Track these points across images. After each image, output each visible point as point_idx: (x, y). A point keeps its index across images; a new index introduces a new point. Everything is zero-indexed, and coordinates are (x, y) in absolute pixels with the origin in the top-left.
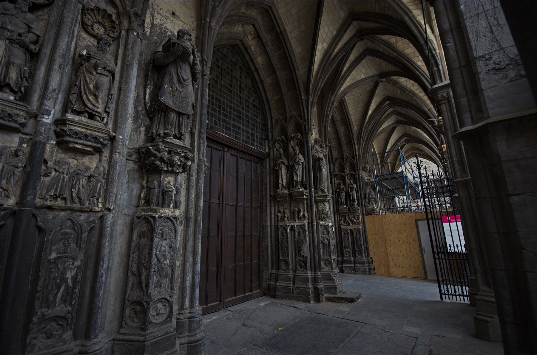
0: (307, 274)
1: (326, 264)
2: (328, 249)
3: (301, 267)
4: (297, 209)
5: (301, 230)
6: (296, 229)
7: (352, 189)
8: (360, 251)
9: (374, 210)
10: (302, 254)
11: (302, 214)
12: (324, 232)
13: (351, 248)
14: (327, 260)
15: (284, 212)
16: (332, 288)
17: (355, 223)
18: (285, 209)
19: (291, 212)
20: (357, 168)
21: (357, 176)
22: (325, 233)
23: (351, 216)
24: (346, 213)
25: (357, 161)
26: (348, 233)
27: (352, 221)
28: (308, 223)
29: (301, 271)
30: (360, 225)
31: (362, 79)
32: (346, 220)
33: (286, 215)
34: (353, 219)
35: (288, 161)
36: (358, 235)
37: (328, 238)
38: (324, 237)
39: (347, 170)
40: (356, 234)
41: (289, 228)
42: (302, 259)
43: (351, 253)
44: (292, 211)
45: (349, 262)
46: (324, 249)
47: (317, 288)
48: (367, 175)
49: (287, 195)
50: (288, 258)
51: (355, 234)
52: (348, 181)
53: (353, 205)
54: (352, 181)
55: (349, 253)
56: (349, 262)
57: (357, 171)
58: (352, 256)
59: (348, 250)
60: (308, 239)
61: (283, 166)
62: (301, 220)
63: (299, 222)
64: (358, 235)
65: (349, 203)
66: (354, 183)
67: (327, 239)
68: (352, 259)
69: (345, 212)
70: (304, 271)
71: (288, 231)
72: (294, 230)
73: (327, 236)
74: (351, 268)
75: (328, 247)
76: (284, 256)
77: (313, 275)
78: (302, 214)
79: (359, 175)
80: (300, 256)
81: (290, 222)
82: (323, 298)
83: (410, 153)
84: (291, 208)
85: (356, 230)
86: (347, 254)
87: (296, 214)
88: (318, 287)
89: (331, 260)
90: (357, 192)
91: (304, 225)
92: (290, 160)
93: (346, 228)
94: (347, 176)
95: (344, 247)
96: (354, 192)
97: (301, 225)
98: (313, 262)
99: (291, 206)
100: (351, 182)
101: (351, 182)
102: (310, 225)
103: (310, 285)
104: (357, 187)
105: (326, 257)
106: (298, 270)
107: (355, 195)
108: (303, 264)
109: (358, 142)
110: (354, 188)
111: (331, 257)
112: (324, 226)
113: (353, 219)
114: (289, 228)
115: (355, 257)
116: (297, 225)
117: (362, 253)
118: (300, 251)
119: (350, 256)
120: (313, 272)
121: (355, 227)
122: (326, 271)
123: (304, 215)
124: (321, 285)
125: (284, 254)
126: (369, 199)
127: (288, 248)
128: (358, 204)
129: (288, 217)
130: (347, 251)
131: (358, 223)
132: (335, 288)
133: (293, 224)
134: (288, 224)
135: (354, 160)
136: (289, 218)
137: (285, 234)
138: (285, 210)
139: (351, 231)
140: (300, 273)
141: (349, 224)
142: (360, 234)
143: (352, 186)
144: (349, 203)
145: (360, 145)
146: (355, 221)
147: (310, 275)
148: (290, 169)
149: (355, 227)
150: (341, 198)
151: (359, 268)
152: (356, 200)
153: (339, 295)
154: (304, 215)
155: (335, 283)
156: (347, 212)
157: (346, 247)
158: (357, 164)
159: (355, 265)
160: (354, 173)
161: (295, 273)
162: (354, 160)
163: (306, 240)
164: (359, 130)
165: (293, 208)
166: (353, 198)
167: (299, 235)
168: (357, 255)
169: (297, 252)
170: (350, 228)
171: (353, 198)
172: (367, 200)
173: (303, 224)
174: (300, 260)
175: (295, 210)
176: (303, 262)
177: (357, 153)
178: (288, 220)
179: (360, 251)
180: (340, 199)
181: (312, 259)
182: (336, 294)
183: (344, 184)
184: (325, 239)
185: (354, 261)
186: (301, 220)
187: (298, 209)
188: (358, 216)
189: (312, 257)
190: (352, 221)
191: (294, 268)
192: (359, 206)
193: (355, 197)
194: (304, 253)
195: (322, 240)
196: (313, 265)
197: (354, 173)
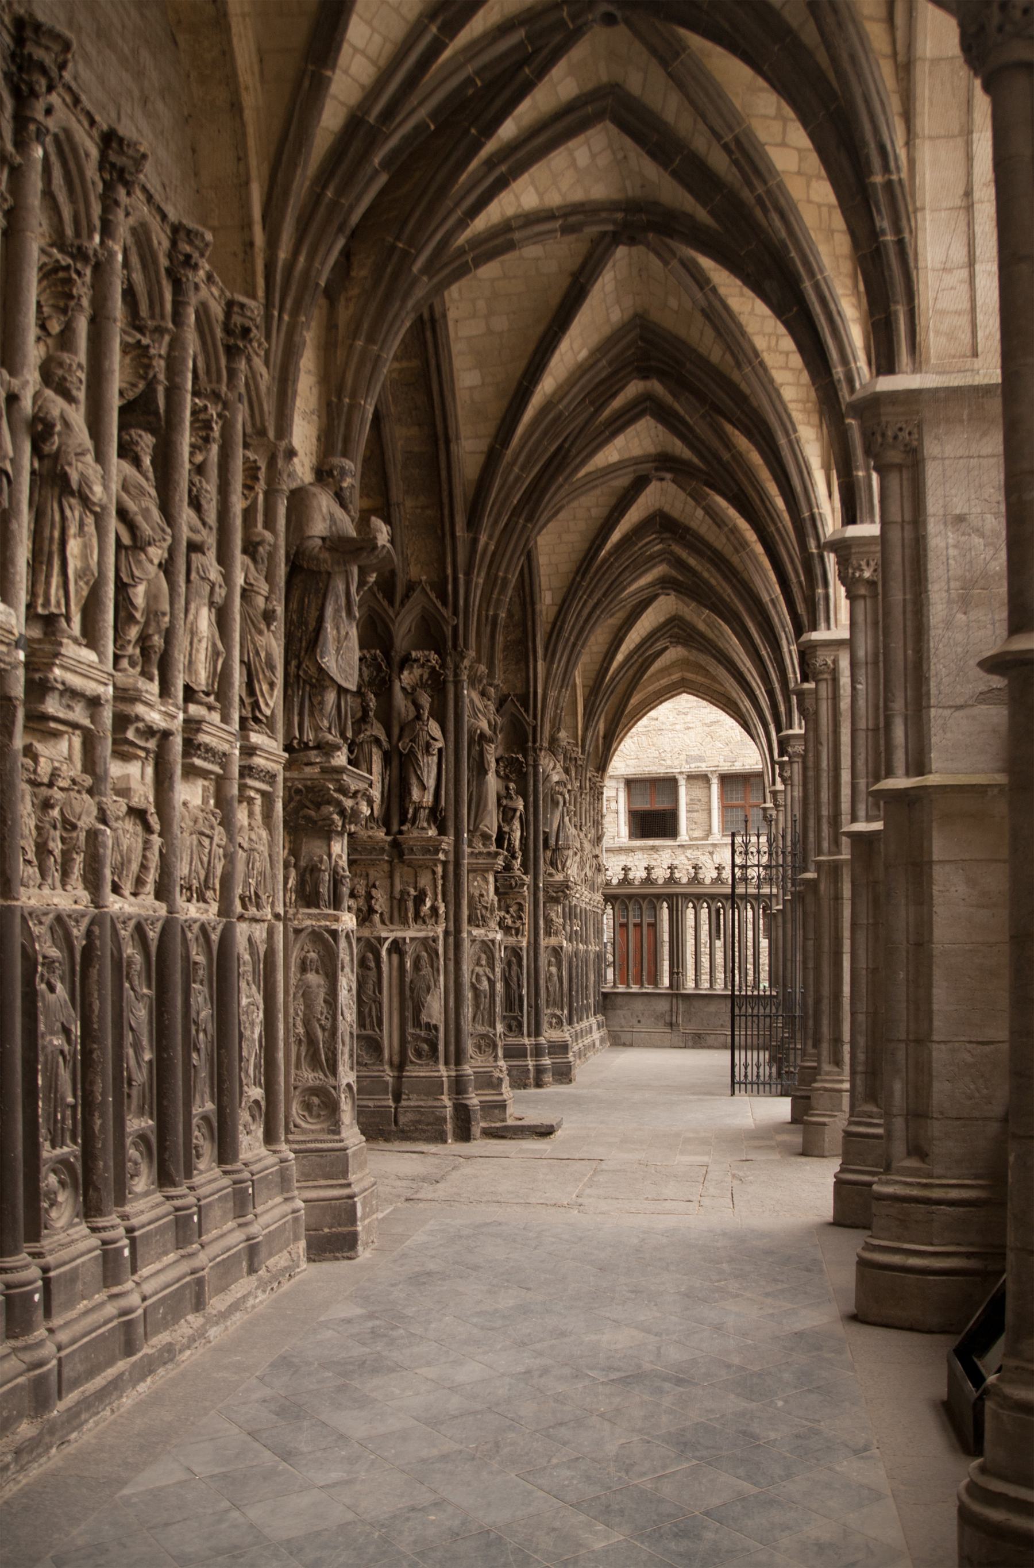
0: (438, 1071)
1: (479, 1047)
2: (487, 1006)
3: (419, 1054)
4: (412, 892)
5: (424, 954)
6: (410, 949)
7: (510, 814)
8: (515, 1018)
9: (568, 887)
10: (424, 1018)
11: (428, 904)
12: (479, 959)
14: (483, 1036)
15: (369, 897)
16: (495, 1107)
18: (374, 886)
19: (392, 897)
21: (531, 769)
22: (484, 962)
25: (535, 717)
28: (446, 933)
29: (421, 1065)
30: (523, 935)
31: (609, 466)
33: (377, 907)
35: (389, 735)
36: (515, 967)
37: (491, 976)
38: (481, 973)
41: (386, 945)
42: (423, 1033)
44: (398, 896)
46: (477, 1006)
47: (466, 1106)
49: (387, 847)
50: (381, 1030)
54: (512, 785)
57: (531, 753)
60: (442, 978)
61: (374, 750)
62: (424, 922)
63: (421, 930)
64: (515, 967)
66: (517, 793)
67: (489, 979)
70: (427, 1065)
71: (384, 953)
72: (401, 954)
73: (487, 970)
75: (487, 1000)
76: (368, 1026)
77: (453, 1074)
78: (428, 904)
79: (536, 767)
80: (417, 1023)
81: (391, 927)
82: (476, 1130)
83: (675, 677)
84: (392, 885)
87: (410, 905)
88: (468, 1102)
89: (495, 1035)
90: (524, 825)
91: (435, 940)
92: (396, 731)
96: (517, 824)
97: (426, 939)
98: (452, 1040)
99: (391, 876)
100: (507, 788)
101: (507, 788)
102: (451, 939)
103: (446, 1101)
104: (525, 807)
105: (482, 1029)
106: (412, 1062)
107: (518, 834)
108: (426, 1047)
109: (546, 649)
110: (515, 810)
111: (495, 1028)
112: (483, 942)
114: (386, 945)
116: (412, 939)
117: (520, 1025)
118: (418, 1009)
120: (452, 1066)
122: (480, 1064)
123: (434, 909)
124: (474, 1099)
125: (368, 1021)
127: (380, 1004)
129: (381, 914)
131: (517, 930)
132: (502, 1106)
133: (399, 934)
134: (384, 935)
135: (527, 711)
136: (386, 917)
137: (372, 964)
138: (374, 892)
140: (417, 1071)
142: (520, 966)
143: (511, 804)
145: (552, 662)
147: (445, 1074)
148: (395, 763)
153: (510, 1122)
154: (434, 909)
155: (502, 1094)
158: (535, 728)
160: (520, 756)
161: (402, 1071)
162: (527, 711)
163: (436, 981)
164: (556, 609)
165: (398, 887)
167: (417, 966)
169: (409, 1014)
173: (431, 934)
174: (417, 1037)
175: (404, 893)
176: (426, 1041)
177: (540, 691)
178: (383, 922)
181: (452, 1033)
182: (504, 1120)
184: (484, 978)
186: (424, 922)
187: (415, 889)
189: (452, 1026)
191: (396, 1059)
192: (526, 873)
193: (517, 843)
194: (430, 1016)
195: (474, 980)
196: (452, 1048)
197: (520, 756)
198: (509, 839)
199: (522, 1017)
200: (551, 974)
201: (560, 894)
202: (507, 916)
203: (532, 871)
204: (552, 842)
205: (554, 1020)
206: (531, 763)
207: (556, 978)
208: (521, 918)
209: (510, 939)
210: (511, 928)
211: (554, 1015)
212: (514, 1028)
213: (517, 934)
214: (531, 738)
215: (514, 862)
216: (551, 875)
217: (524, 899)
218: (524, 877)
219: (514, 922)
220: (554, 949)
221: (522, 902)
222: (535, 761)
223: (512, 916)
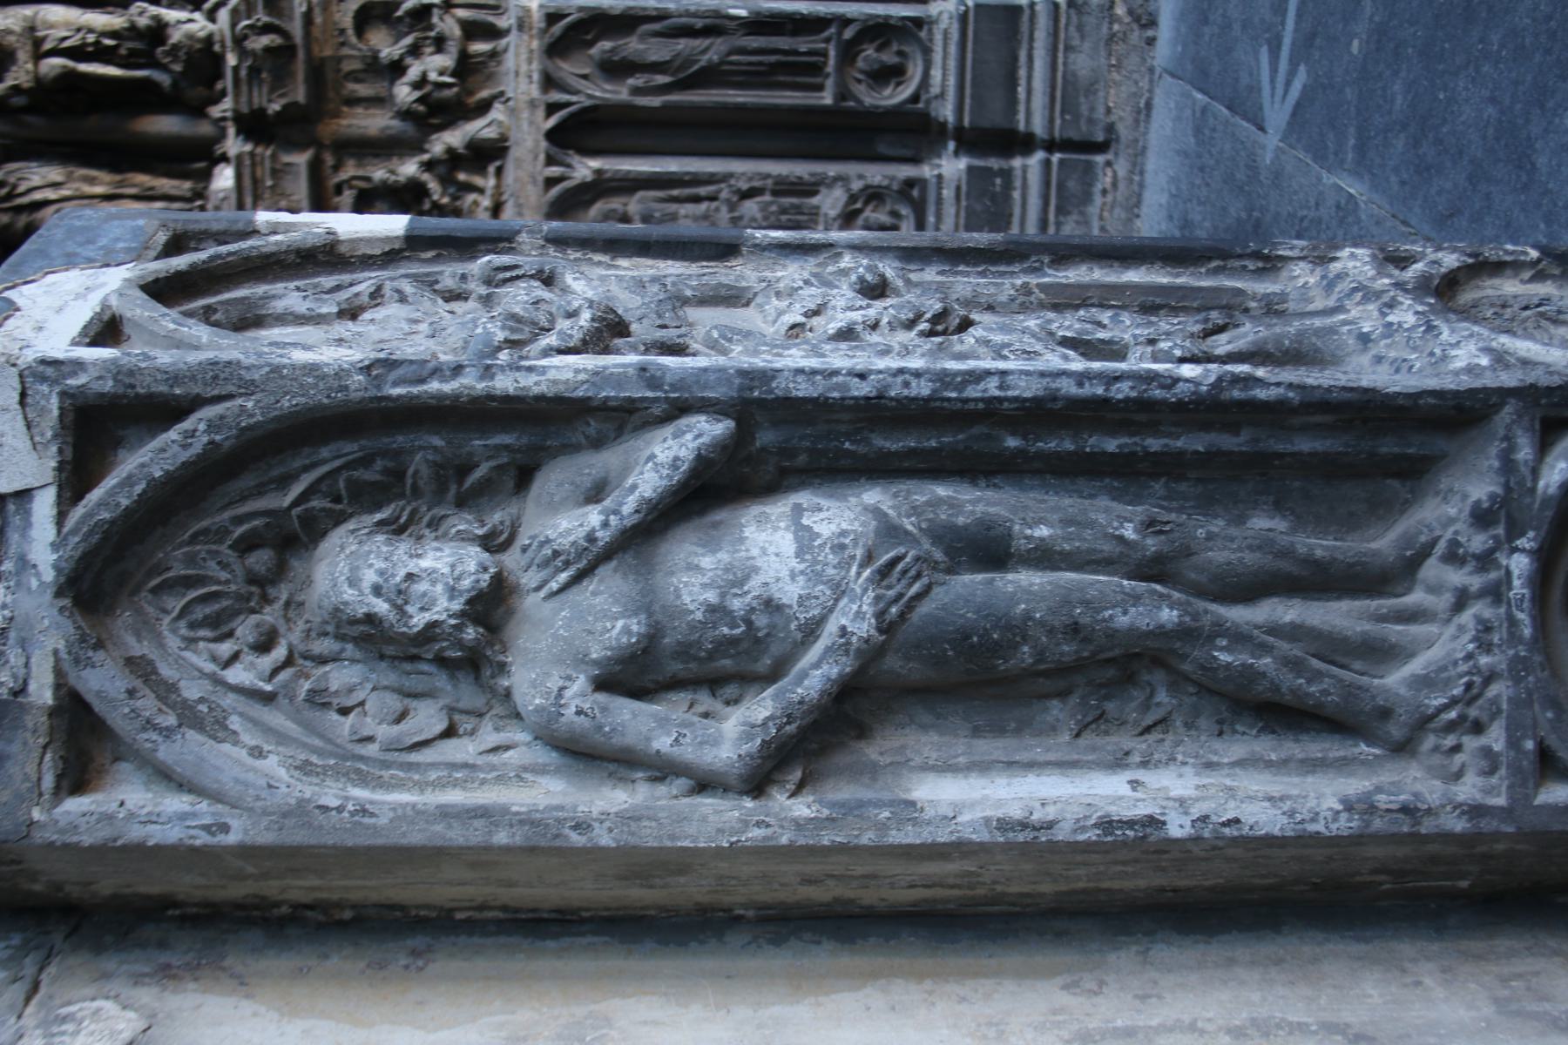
8: (849, 53)
13: (800, 169)
17: (466, 68)
23: (375, 122)
26: (600, 187)
36: (633, 46)
40: (615, 69)
43: (876, 174)
51: (618, 92)
58: (905, 171)
64: (633, 46)
65: (166, 125)
68: (951, 166)
85: (568, 69)
113: (404, 93)
141: (487, 154)
144: (166, 125)
146: (435, 65)
151: (1067, 92)
156: (301, 159)
159: (1024, 143)
166: (99, 53)
168: (894, 96)
171: (99, 53)
179: (849, 53)
185: (972, 140)
198: (77, 53)
199: (845, 21)
202: (414, 72)
209: (510, 61)
210: (464, 58)
212: (889, 58)
213: (493, 33)
215: (176, 36)
219: (440, 44)
223: (415, 51)
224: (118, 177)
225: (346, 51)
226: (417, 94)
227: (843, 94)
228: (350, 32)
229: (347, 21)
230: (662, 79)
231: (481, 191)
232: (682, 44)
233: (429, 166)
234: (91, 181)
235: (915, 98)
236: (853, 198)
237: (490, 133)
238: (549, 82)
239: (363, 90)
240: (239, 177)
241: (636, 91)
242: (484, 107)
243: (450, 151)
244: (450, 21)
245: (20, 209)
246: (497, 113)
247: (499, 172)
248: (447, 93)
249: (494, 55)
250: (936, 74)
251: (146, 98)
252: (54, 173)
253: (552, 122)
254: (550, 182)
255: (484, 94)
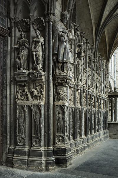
8: (38, 138)
20: (48, 10)
23: (31, 87)
24: (25, 81)
26: (24, 111)
27: (32, 93)
30: (42, 100)
32: (24, 91)
34: (33, 90)
36: (38, 114)
39: (35, 14)
40: (36, 113)
45: (23, 153)
48: (63, 26)
51: (33, 113)
52: (33, 33)
53: (35, 69)
55: (24, 140)
56: (23, 153)
57: (47, 16)
59: (23, 136)
64: (38, 114)
65: (31, 66)
66: (42, 35)
69: (23, 79)
74: (23, 162)
86: (20, 141)
93: (23, 104)
94: (33, 24)
95: (17, 132)
104: (45, 41)
107: (41, 53)
115: (31, 145)
117: (40, 141)
119: (24, 145)
121: (36, 102)
126: (64, 63)
128: (44, 69)
130: (22, 138)
131: (40, 97)
139: (29, 108)
142: (40, 114)
146: (36, 93)
149: (36, 102)
150: (20, 59)
152: (41, 62)
156: (26, 79)
157: (20, 131)
160: (42, 18)
170: (28, 103)
172: (60, 65)
179: (38, 138)
180: (18, 60)
183: (28, 37)
188: (42, 87)
190: (32, 93)
192: (44, 71)
197: (42, 18)
199: (41, 137)
200: (59, 118)
201: (63, 81)
202: (35, 91)
203: (47, 70)
204: (61, 58)
205: (61, 138)
206: (47, 21)
207: (61, 120)
208: (41, 91)
211: (61, 136)
213: (40, 99)
214: (46, 9)
216: (60, 74)
217: (43, 83)
218: (43, 73)
219: (38, 93)
220: (61, 106)
221: (42, 84)
222: (49, 19)
223: (38, 91)
224: (26, 60)
225: (38, 84)
226: (33, 91)
227: (33, 137)
228: (39, 84)
229: (40, 84)
230: (35, 117)
231: (24, 98)
232: (38, 120)
233: (27, 93)
234: (25, 57)
235: (33, 145)
236: (24, 138)
237: (29, 99)
238: (34, 105)
239: (35, 85)
240: (24, 73)
241: (33, 115)
242: (32, 99)
243: (28, 95)
244: (40, 95)
245: (21, 50)
246: (31, 99)
247: (26, 100)
248: (33, 94)
249: (38, 99)
250: (36, 147)
251: (33, 63)
252: (25, 54)
253: (30, 106)
254: (24, 105)
255: (34, 98)
